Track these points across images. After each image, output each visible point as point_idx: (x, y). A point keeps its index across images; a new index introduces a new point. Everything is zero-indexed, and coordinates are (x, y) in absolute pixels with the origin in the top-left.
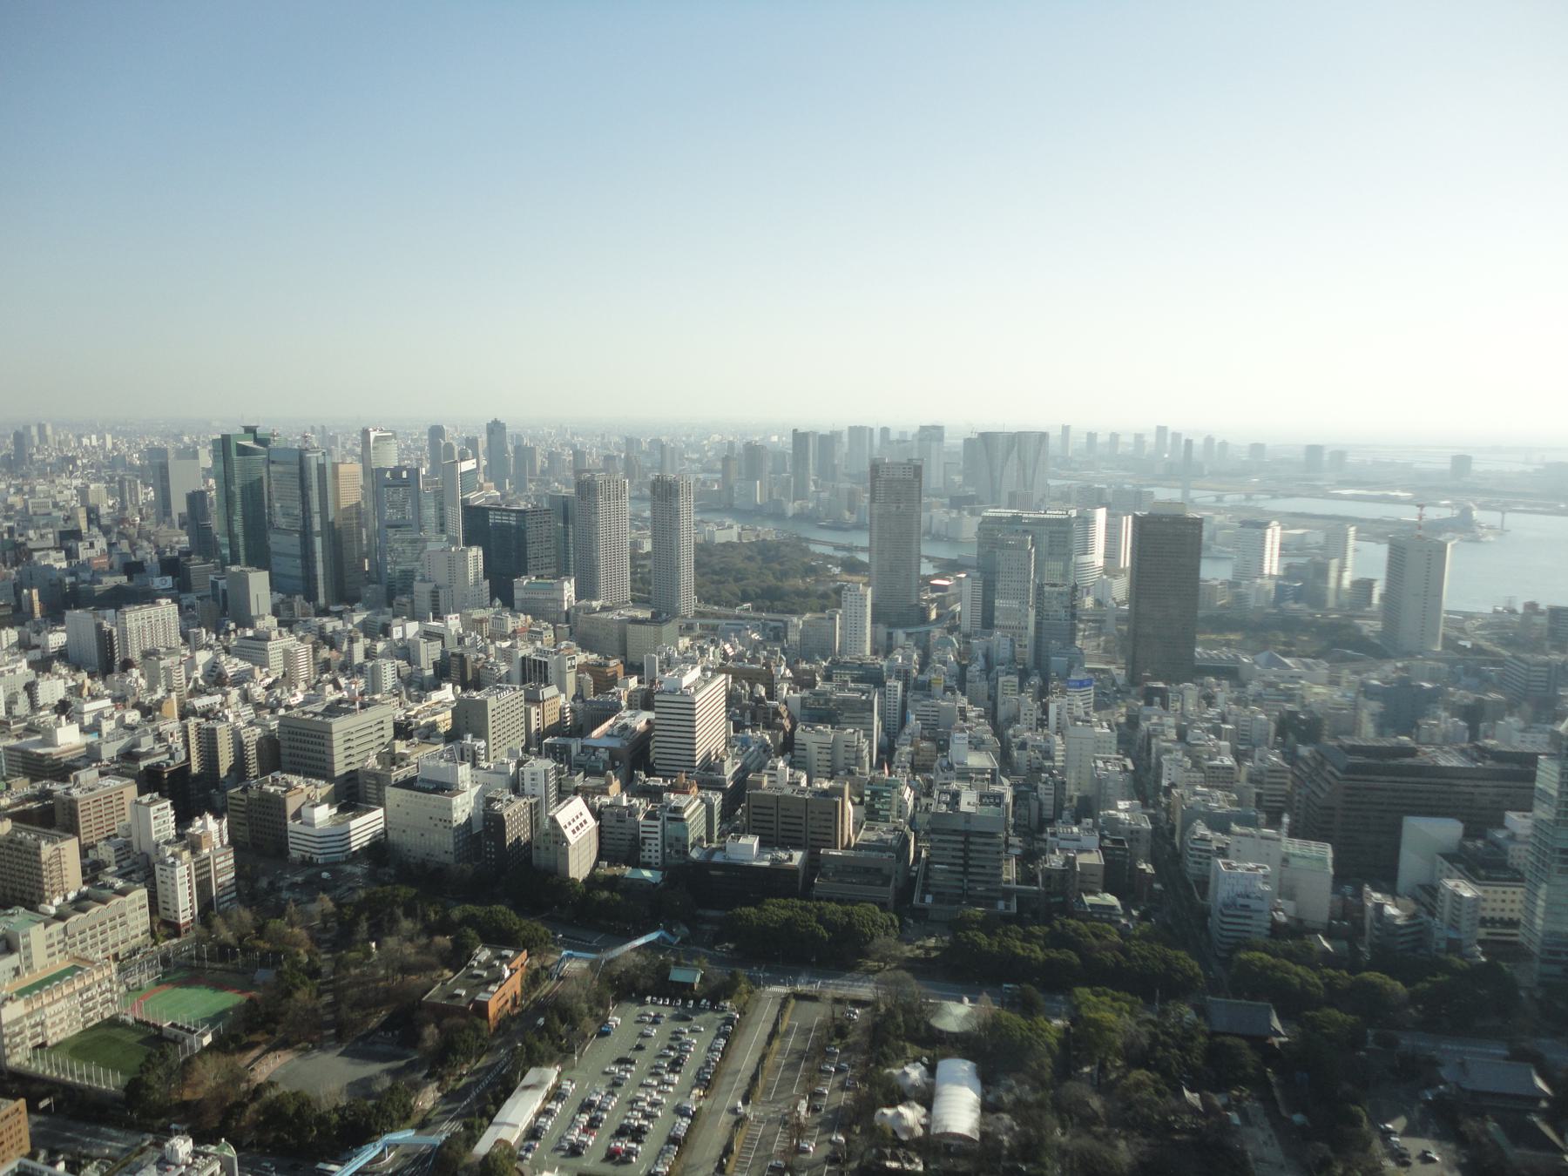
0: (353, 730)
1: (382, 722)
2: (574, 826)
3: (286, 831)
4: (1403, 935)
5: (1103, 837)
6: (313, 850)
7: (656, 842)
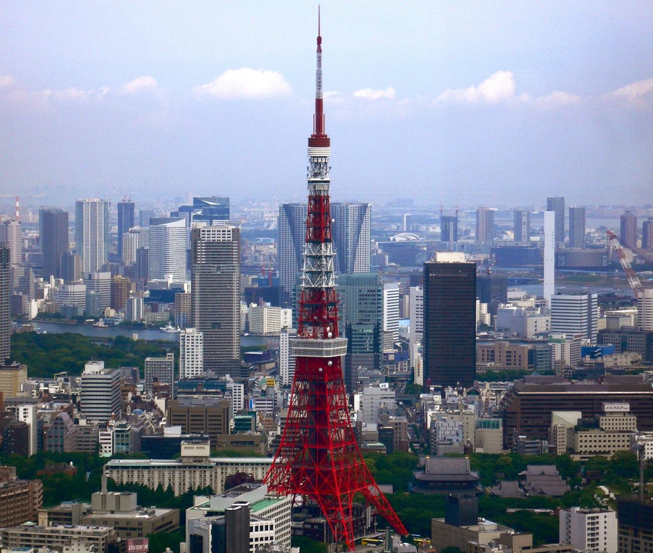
4: (528, 448)
5: (379, 425)
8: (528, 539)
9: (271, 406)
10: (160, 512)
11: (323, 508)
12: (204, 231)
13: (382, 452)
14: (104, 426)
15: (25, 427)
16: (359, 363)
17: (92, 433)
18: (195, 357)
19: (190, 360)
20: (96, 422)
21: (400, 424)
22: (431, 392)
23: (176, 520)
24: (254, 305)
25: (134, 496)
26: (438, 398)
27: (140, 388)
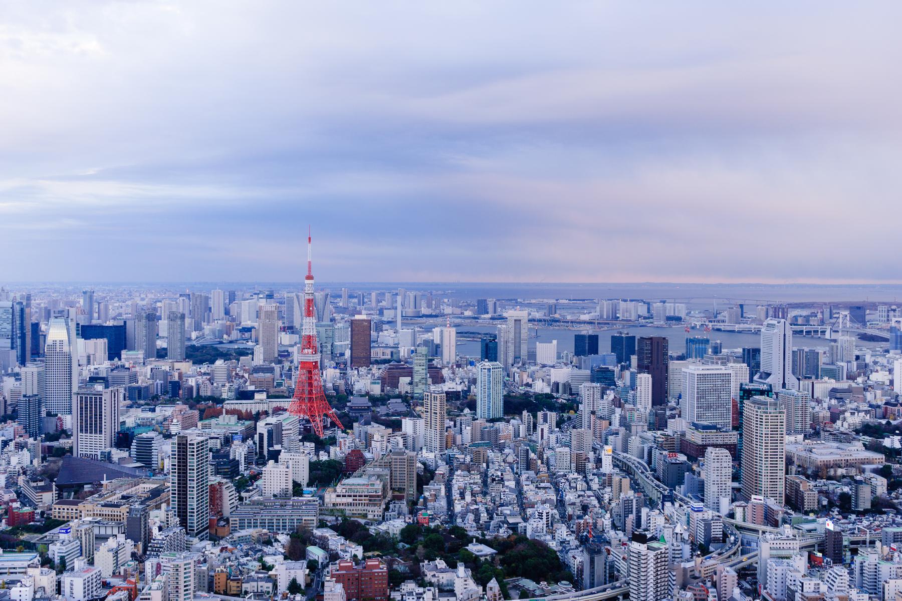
8: (390, 430)
10: (247, 423)
11: (311, 420)
14: (224, 386)
15: (192, 387)
20: (220, 385)
23: (253, 426)
24: (283, 333)
25: (236, 416)
26: (356, 372)
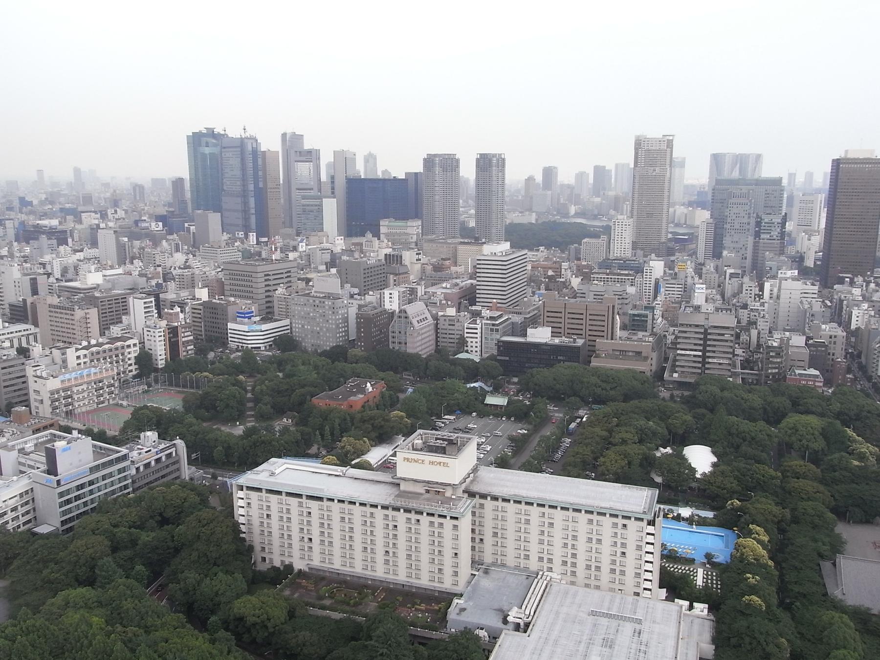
0: (270, 273)
1: (289, 272)
2: (418, 319)
3: (227, 329)
6: (244, 341)
7: (476, 340)
9: (680, 289)
12: (644, 141)
13: (817, 384)
16: (766, 249)
17: (457, 324)
18: (623, 239)
19: (619, 242)
21: (835, 337)
22: (846, 283)
24: (691, 209)
27: (565, 266)
